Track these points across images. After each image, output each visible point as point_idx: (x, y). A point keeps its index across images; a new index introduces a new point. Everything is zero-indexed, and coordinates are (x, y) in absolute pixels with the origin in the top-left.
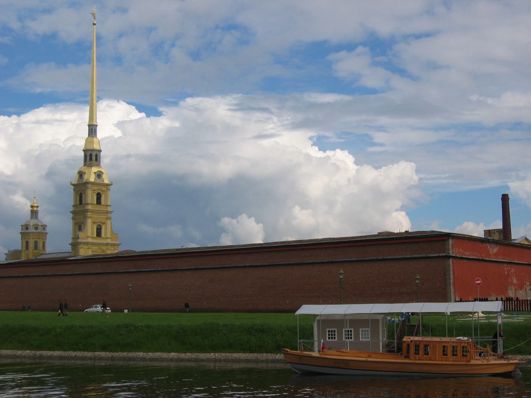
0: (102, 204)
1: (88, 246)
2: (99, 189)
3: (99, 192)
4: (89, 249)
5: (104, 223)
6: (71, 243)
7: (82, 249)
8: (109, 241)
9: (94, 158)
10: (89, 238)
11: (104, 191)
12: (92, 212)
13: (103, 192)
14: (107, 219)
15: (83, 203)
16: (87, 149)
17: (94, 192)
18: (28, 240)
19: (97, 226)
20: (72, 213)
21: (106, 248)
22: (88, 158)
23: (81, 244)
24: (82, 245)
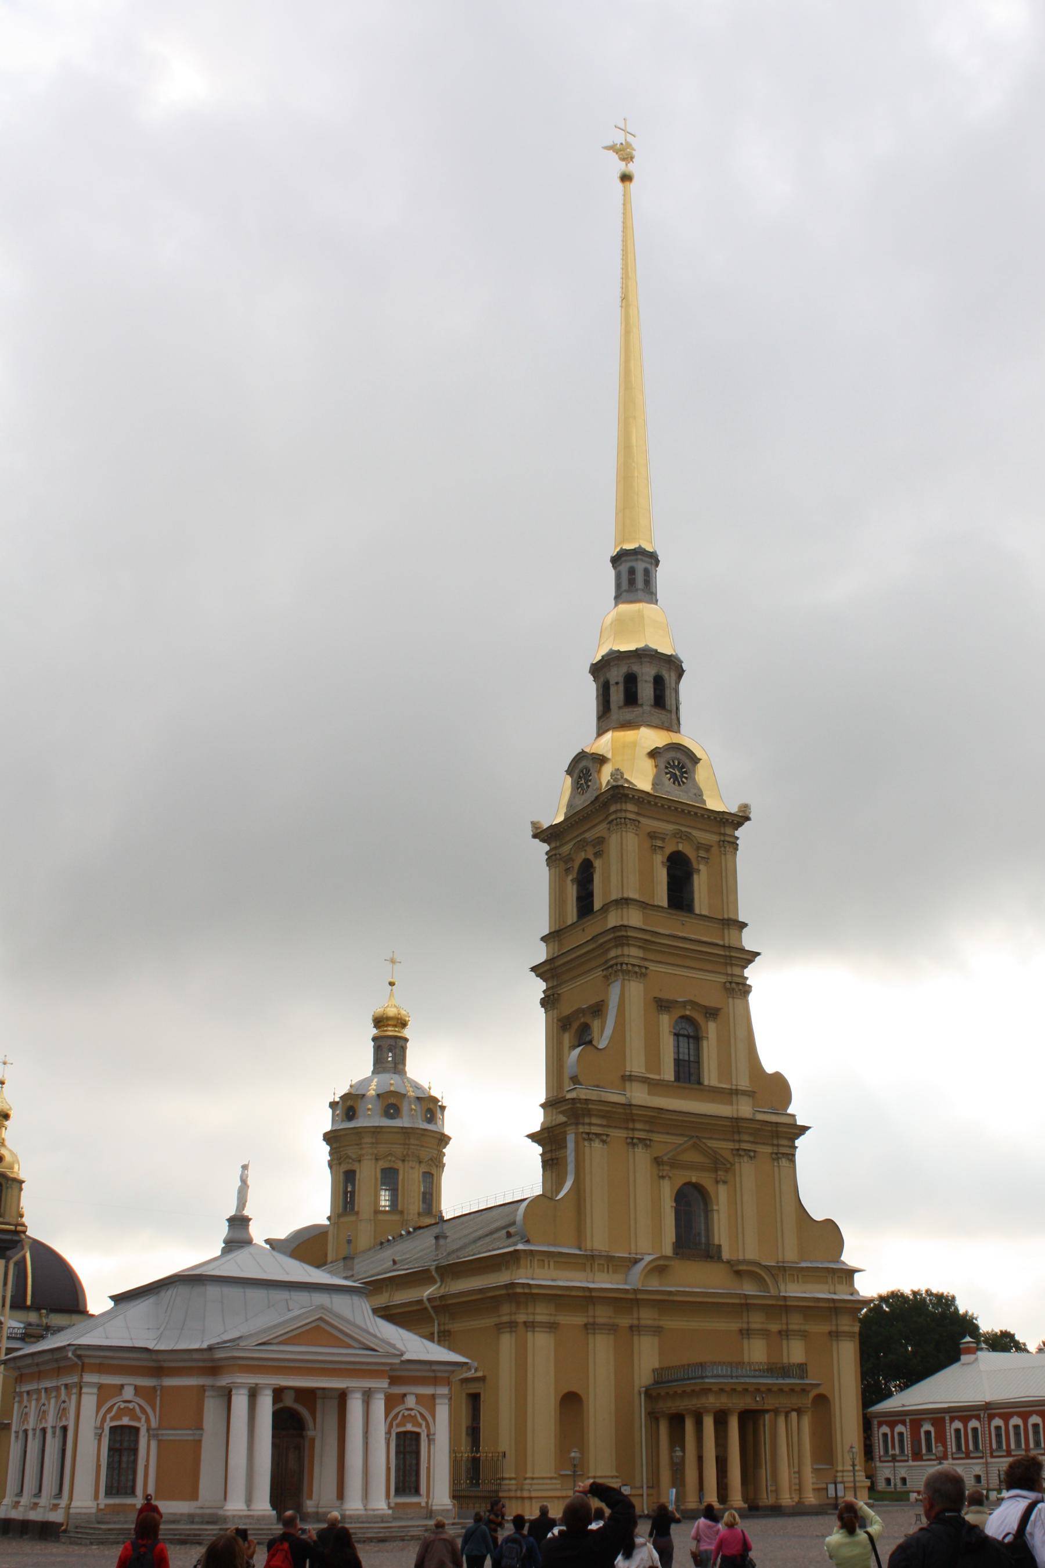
0: (697, 911)
1: (631, 1126)
2: (680, 836)
3: (680, 848)
4: (634, 1145)
5: (712, 1013)
6: (537, 1128)
7: (597, 1144)
8: (744, 1109)
9: (646, 691)
10: (636, 1085)
11: (708, 848)
12: (645, 945)
13: (702, 854)
14: (726, 989)
15: (597, 905)
17: (654, 849)
18: (355, 1166)
19: (676, 1023)
20: (537, 976)
21: (731, 1145)
22: (617, 695)
23: (589, 1113)
24: (594, 1120)
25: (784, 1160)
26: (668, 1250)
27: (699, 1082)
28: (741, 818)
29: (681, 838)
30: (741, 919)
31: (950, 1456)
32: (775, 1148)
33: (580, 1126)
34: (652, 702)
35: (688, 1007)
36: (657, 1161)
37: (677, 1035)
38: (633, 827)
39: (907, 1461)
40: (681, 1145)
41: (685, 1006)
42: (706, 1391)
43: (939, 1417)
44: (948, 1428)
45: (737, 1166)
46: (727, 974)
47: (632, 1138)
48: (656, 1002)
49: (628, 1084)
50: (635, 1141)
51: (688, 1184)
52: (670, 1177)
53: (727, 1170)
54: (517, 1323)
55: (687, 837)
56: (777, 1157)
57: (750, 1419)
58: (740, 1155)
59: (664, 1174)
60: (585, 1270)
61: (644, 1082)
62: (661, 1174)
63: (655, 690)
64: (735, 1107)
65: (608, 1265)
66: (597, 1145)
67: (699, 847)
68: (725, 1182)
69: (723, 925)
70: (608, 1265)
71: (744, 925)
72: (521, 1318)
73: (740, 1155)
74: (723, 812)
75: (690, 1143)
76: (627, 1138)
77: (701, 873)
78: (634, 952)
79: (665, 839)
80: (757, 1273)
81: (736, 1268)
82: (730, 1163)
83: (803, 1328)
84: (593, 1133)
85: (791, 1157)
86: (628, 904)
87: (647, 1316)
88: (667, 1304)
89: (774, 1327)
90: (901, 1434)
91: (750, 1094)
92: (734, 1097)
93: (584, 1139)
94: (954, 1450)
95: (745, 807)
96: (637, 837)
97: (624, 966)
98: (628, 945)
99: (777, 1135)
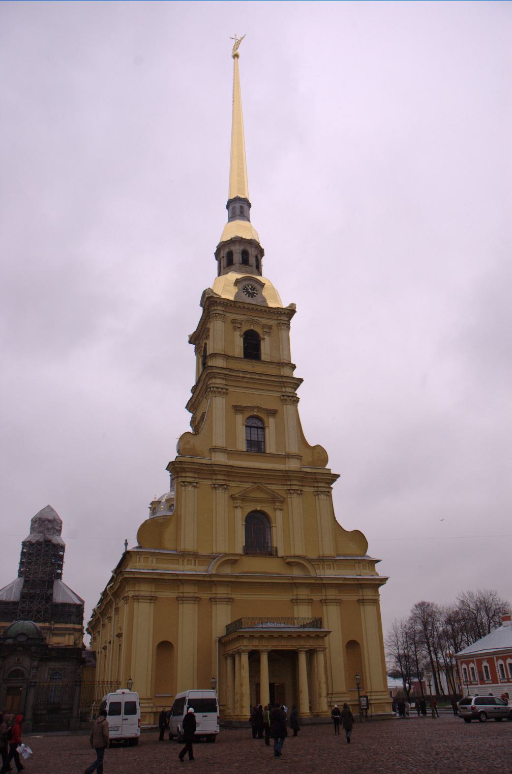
1: (214, 477)
3: (252, 328)
4: (216, 488)
5: (273, 413)
7: (190, 488)
8: (293, 465)
9: (237, 258)
11: (270, 327)
12: (226, 377)
13: (267, 330)
14: (282, 400)
16: (220, 243)
17: (235, 328)
21: (285, 488)
22: (224, 262)
23: (184, 470)
24: (188, 474)
25: (322, 496)
26: (239, 550)
27: (264, 452)
28: (291, 312)
29: (252, 322)
30: (293, 362)
31: (499, 681)
32: (316, 489)
33: (179, 478)
34: (241, 262)
35: (255, 410)
36: (232, 497)
37: (246, 426)
38: (221, 318)
39: (477, 684)
40: (248, 488)
41: (253, 410)
42: (241, 637)
43: (491, 657)
44: (496, 664)
45: (289, 499)
46: (282, 392)
47: (214, 484)
48: (234, 408)
49: (213, 454)
50: (216, 486)
51: (255, 512)
52: (242, 507)
53: (282, 502)
54: (128, 597)
55: (257, 323)
56: (317, 493)
57: (276, 657)
58: (291, 493)
59: (237, 505)
60: (179, 564)
61: (224, 452)
62: (235, 505)
63: (243, 257)
64: (287, 465)
65: (195, 561)
66: (190, 489)
67: (264, 326)
68: (281, 510)
69: (280, 366)
70: (195, 561)
71: (294, 367)
72: (131, 594)
73: (291, 493)
74: (278, 308)
75: (256, 486)
76: (211, 485)
77: (266, 339)
78: (219, 381)
79: (241, 323)
80: (303, 564)
81: (286, 561)
82: (283, 497)
83: (338, 597)
84: (187, 482)
85: (328, 494)
86: (215, 357)
87: (222, 592)
88: (235, 584)
89: (317, 598)
90: (472, 668)
91: (298, 457)
92: (287, 460)
93: (182, 486)
94: (501, 677)
95: (293, 305)
96: (223, 323)
97: (212, 389)
98: (215, 378)
99: (317, 480)
